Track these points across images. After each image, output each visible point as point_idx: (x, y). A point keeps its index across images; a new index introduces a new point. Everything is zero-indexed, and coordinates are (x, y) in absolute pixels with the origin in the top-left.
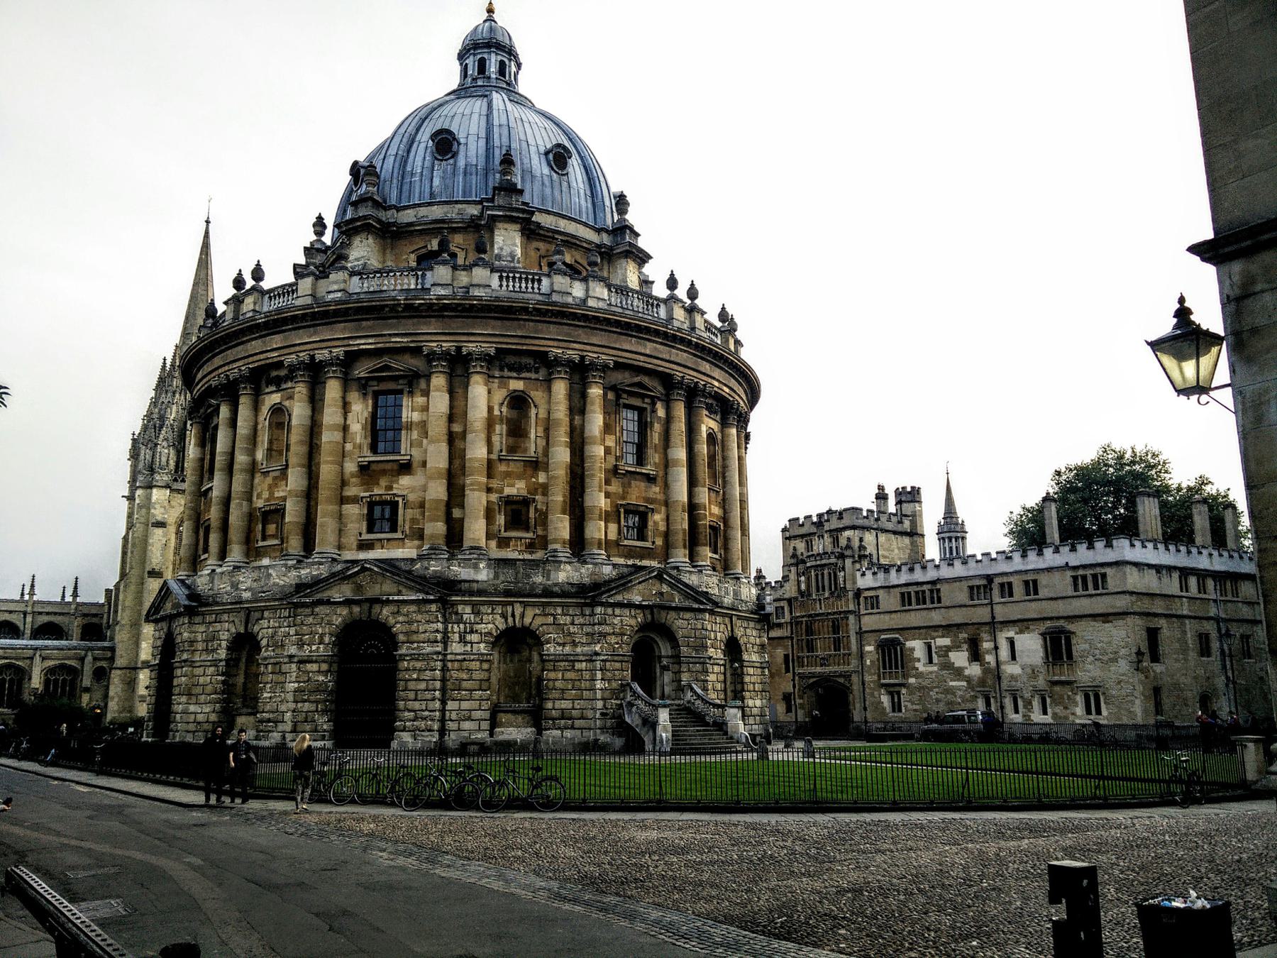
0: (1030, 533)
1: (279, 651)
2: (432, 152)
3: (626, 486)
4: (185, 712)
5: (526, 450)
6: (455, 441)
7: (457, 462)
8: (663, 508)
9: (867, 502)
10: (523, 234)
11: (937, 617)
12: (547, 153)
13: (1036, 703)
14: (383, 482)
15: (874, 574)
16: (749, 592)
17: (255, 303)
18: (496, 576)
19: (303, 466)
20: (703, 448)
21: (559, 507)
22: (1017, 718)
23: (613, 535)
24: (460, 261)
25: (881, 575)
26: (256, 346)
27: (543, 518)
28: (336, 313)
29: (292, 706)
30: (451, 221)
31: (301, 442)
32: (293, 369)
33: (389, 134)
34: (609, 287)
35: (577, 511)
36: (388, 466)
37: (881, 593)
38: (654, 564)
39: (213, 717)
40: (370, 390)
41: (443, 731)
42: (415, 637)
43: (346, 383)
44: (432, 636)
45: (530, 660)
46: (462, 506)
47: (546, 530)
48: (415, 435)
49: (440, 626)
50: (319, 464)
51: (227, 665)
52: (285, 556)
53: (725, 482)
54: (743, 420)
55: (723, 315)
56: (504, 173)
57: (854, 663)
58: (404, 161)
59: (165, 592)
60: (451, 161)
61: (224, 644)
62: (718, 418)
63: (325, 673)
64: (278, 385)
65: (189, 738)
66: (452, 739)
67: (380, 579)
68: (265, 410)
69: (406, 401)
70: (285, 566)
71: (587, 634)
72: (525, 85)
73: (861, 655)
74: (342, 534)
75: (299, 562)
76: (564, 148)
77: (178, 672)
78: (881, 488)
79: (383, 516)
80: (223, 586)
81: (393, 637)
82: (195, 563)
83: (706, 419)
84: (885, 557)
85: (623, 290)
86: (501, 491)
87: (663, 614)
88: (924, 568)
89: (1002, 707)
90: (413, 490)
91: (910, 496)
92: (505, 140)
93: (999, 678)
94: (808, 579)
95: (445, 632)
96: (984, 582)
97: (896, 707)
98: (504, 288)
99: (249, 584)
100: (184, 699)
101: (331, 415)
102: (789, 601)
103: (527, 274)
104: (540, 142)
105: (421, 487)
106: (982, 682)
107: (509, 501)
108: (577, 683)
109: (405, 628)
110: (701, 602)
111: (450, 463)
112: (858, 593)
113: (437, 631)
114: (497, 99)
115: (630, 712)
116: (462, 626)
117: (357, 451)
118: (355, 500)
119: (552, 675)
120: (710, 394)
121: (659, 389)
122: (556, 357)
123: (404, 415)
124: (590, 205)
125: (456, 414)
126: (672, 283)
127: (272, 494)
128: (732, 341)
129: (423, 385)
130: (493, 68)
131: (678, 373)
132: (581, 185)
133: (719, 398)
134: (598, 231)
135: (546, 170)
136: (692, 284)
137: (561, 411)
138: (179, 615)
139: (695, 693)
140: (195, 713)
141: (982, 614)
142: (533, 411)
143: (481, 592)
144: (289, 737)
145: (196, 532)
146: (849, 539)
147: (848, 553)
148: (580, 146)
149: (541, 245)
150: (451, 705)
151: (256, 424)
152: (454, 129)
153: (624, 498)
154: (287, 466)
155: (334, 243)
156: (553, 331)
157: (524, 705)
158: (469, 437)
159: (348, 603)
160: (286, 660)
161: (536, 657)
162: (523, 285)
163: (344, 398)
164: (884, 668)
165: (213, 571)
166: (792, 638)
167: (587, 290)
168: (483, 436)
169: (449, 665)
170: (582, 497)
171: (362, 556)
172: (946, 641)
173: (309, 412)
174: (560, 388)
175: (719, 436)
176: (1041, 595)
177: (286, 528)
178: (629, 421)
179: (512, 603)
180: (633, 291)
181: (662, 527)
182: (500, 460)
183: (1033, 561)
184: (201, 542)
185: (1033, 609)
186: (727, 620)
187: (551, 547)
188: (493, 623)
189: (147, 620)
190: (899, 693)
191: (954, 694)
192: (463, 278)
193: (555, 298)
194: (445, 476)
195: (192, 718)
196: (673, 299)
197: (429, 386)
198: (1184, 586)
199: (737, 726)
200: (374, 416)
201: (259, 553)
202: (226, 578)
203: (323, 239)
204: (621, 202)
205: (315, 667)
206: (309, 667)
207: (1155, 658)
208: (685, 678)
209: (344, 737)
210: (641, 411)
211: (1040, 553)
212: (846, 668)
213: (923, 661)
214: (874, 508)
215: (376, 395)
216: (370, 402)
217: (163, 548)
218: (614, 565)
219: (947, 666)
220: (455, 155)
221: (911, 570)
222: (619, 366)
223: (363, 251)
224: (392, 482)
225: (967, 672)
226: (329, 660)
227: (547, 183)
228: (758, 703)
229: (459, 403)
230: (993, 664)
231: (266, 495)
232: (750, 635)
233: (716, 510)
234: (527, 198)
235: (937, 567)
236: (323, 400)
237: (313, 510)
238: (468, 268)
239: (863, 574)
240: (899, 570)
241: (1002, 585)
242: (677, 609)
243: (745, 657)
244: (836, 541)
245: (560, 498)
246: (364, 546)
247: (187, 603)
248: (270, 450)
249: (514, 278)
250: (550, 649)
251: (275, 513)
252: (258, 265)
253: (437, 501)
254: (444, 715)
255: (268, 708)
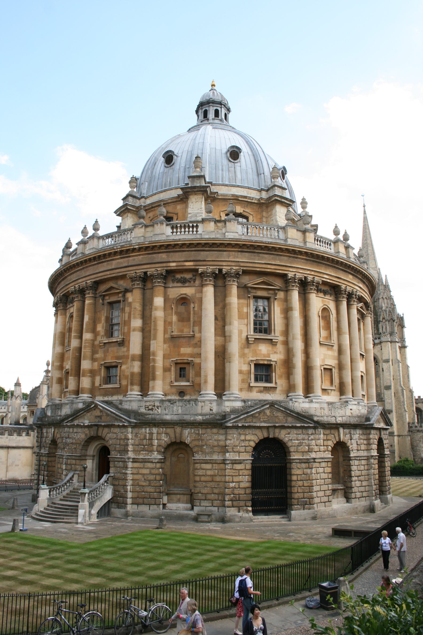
131: (131, 272)
132: (183, 165)
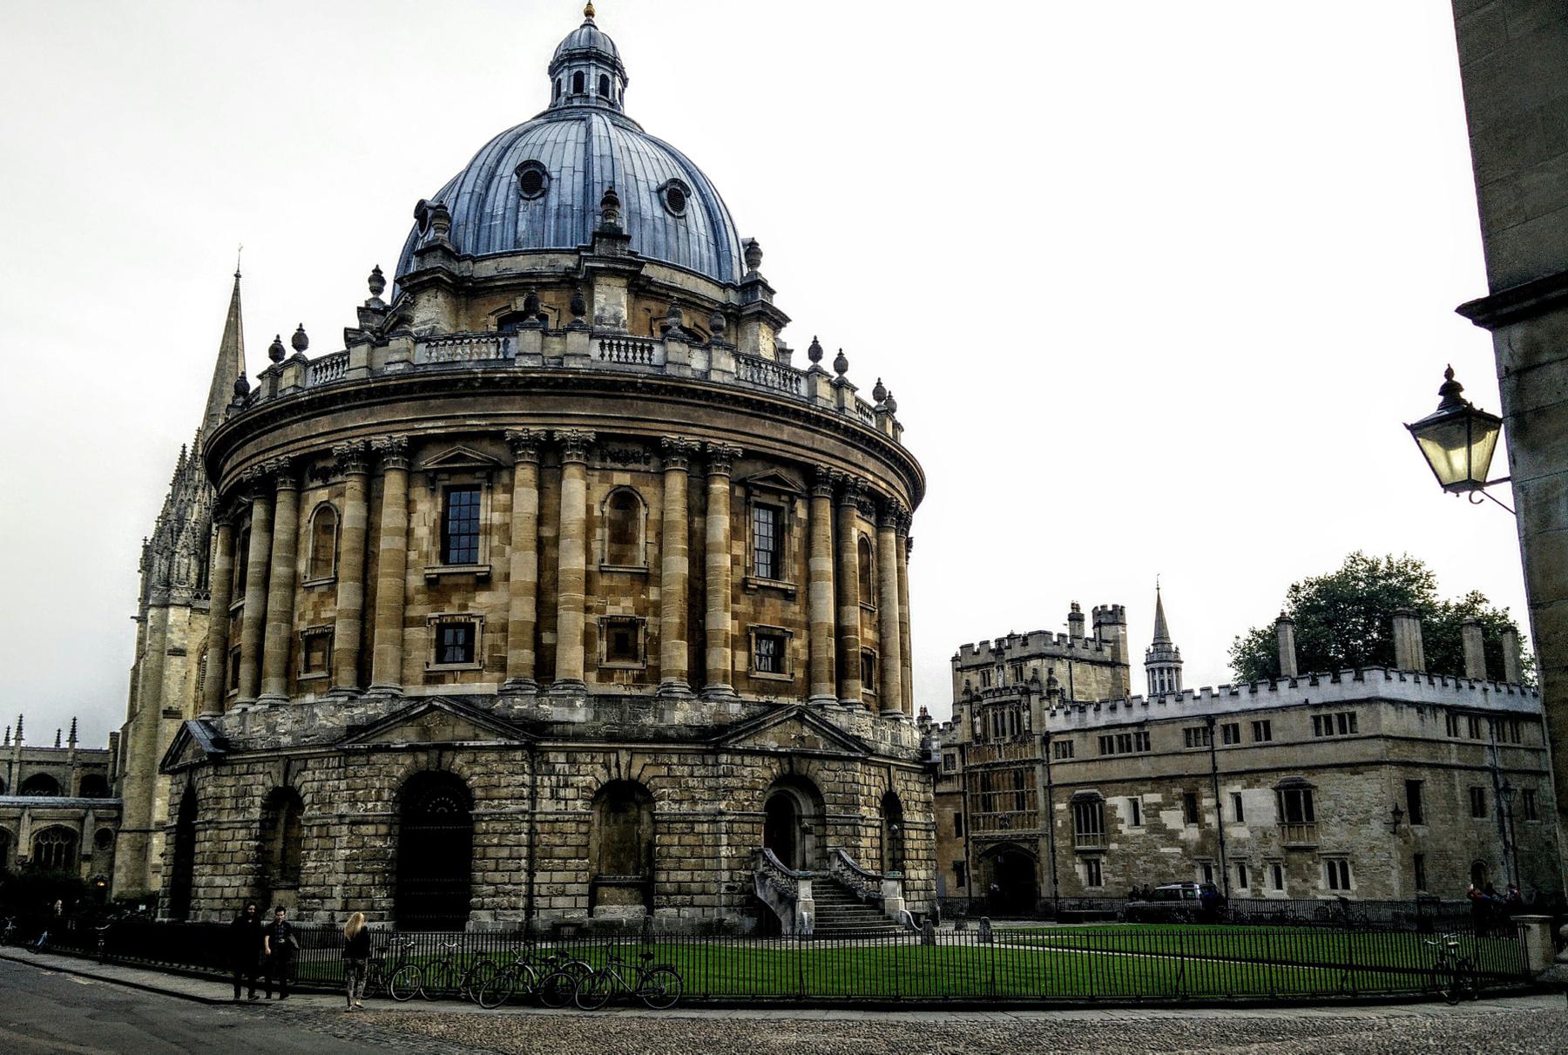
0: (1260, 663)
1: (326, 810)
2: (517, 189)
3: (758, 605)
4: (209, 886)
5: (633, 560)
6: (546, 549)
7: (548, 575)
8: (804, 632)
9: (1058, 625)
10: (629, 292)
11: (1144, 768)
12: (659, 191)
13: (1268, 875)
14: (456, 600)
15: (1067, 713)
16: (911, 737)
17: (296, 377)
18: (597, 717)
19: (356, 579)
20: (853, 558)
21: (674, 631)
22: (1245, 893)
23: (741, 666)
24: (552, 325)
25: (1075, 715)
26: (297, 430)
27: (655, 644)
28: (398, 389)
29: (343, 878)
30: (540, 275)
31: (353, 550)
32: (343, 459)
33: (462, 166)
34: (737, 356)
35: (698, 636)
36: (462, 580)
37: (1075, 737)
38: (793, 701)
39: (245, 892)
40: (440, 484)
41: (530, 909)
42: (495, 793)
43: (410, 476)
44: (517, 791)
45: (638, 821)
46: (554, 630)
47: (658, 658)
48: (495, 541)
49: (527, 779)
50: (376, 577)
51: (262, 827)
52: (333, 691)
53: (881, 600)
54: (904, 523)
55: (879, 392)
56: (606, 215)
57: (1042, 824)
58: (482, 200)
59: (184, 736)
60: (541, 201)
61: (258, 801)
62: (873, 520)
63: (384, 837)
64: (325, 479)
65: (214, 918)
66: (542, 920)
67: (452, 720)
68: (309, 510)
69: (484, 499)
70: (335, 704)
71: (710, 789)
72: (632, 106)
73: (1051, 815)
74: (404, 664)
75: (352, 699)
76: (681, 184)
77: (201, 836)
78: (1075, 607)
79: (456, 641)
80: (257, 729)
81: (468, 792)
82: (221, 701)
83: (858, 522)
84: (1079, 692)
85: (754, 361)
86: (603, 611)
87: (805, 763)
88: (1129, 706)
89: (1226, 880)
90: (493, 609)
91: (1111, 617)
92: (607, 174)
93: (1222, 843)
94: (985, 721)
95: (533, 787)
96: (1203, 724)
97: (1094, 879)
98: (607, 358)
99: (289, 726)
100: (208, 869)
101: (391, 516)
102: (961, 747)
103: (635, 340)
104: (651, 177)
105: (504, 606)
106: (1201, 848)
107: (612, 624)
108: (698, 850)
109: (483, 781)
110: (852, 748)
111: (540, 576)
112: (1047, 738)
113: (523, 785)
114: (598, 122)
115: (763, 886)
116: (554, 778)
117: (423, 561)
118: (421, 622)
119: (666, 840)
120: (862, 489)
121: (797, 483)
122: (671, 444)
123: (482, 516)
124: (713, 255)
125: (547, 515)
126: (815, 352)
127: (317, 614)
128: (889, 425)
129: (505, 479)
130: (592, 85)
132: (702, 231)
133: (873, 494)
134: (725, 287)
135: (659, 212)
136: (841, 354)
137: (677, 512)
138: (202, 764)
139: (844, 861)
140: (223, 887)
141: (1201, 764)
142: (643, 511)
143: (577, 737)
144: (339, 916)
145: (223, 661)
146: (1035, 671)
147: (1034, 687)
148: (701, 181)
149: (653, 305)
150: (540, 877)
151: (298, 527)
152: (544, 160)
153: (755, 620)
154: (336, 579)
155: (395, 302)
156: (667, 412)
157: (631, 877)
158: (563, 543)
159: (412, 749)
160: (335, 821)
161: (646, 817)
162: (630, 355)
163: (407, 495)
164: (1080, 831)
165: (245, 710)
166: (964, 794)
167: (710, 361)
168: (580, 542)
169: (538, 827)
170: (703, 618)
171: (430, 691)
172: (1156, 798)
173: (363, 512)
174: (676, 483)
175: (874, 543)
176: (1274, 741)
177: (335, 656)
178: (761, 523)
179: (615, 750)
180: (766, 362)
181: (803, 656)
182: (602, 572)
183: (1265, 698)
184: (230, 674)
185: (1264, 758)
186: (884, 771)
187: (664, 680)
188: (592, 774)
189: (163, 772)
190: (1097, 862)
191: (1166, 863)
192: (556, 346)
193: (670, 370)
194: (533, 592)
195: (218, 892)
196: (816, 372)
197: (512, 479)
198: (1452, 729)
199: (896, 903)
200: (444, 518)
201: (302, 688)
202: (260, 719)
203: (381, 297)
204: (752, 251)
205: (371, 829)
206: (364, 829)
207: (1416, 819)
208: (831, 842)
209: (408, 916)
210: (777, 511)
211: (1273, 688)
212: (1032, 831)
213: (1127, 822)
214: (1066, 631)
215: (447, 491)
216: (440, 500)
217: (182, 682)
218: (744, 703)
219: (1158, 828)
220: (545, 193)
221: (1113, 709)
222: (749, 455)
223: (430, 312)
224: (467, 599)
225: (1182, 836)
226: (389, 821)
227: (660, 226)
228: (922, 874)
229: (551, 501)
230: (1215, 826)
231: (310, 615)
232: (912, 790)
233: (870, 634)
234: (634, 246)
235: (1145, 705)
236: (381, 498)
237: (368, 635)
238: (561, 333)
239: (1053, 714)
240: (1098, 708)
241: (1226, 728)
242: (821, 757)
243: (907, 817)
244: (1019, 673)
245: (676, 620)
246: (432, 679)
247: (211, 750)
248: (315, 559)
249: (619, 345)
250: (664, 807)
251: (321, 638)
252: (300, 329)
253: (524, 623)
254: (531, 889)
255: (312, 880)
